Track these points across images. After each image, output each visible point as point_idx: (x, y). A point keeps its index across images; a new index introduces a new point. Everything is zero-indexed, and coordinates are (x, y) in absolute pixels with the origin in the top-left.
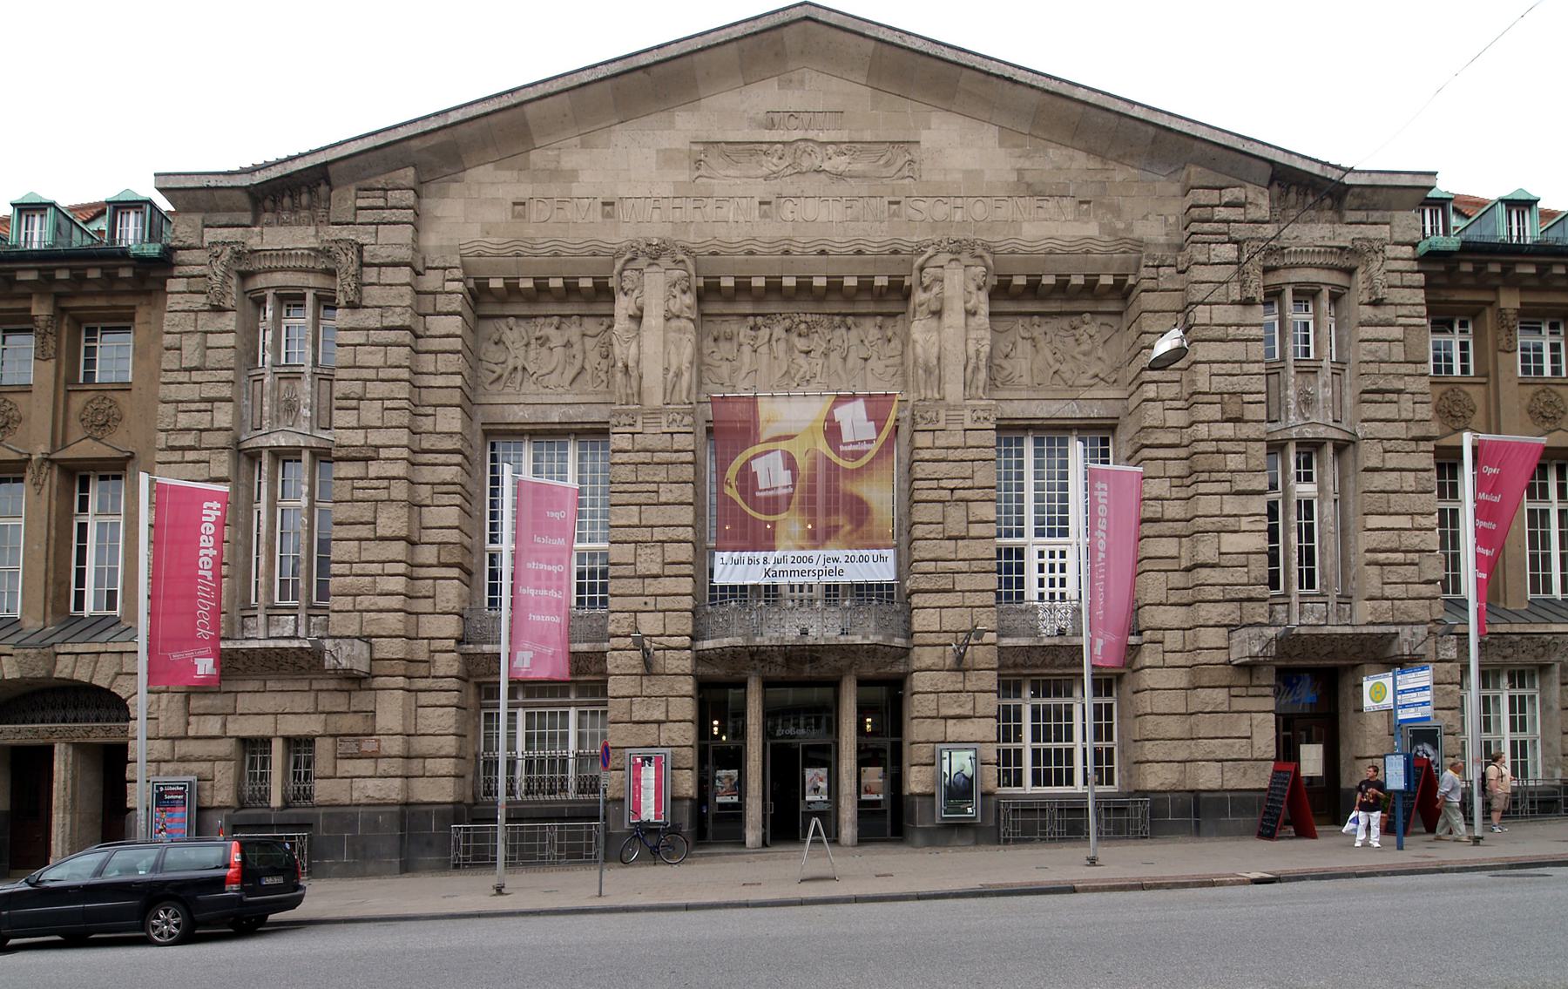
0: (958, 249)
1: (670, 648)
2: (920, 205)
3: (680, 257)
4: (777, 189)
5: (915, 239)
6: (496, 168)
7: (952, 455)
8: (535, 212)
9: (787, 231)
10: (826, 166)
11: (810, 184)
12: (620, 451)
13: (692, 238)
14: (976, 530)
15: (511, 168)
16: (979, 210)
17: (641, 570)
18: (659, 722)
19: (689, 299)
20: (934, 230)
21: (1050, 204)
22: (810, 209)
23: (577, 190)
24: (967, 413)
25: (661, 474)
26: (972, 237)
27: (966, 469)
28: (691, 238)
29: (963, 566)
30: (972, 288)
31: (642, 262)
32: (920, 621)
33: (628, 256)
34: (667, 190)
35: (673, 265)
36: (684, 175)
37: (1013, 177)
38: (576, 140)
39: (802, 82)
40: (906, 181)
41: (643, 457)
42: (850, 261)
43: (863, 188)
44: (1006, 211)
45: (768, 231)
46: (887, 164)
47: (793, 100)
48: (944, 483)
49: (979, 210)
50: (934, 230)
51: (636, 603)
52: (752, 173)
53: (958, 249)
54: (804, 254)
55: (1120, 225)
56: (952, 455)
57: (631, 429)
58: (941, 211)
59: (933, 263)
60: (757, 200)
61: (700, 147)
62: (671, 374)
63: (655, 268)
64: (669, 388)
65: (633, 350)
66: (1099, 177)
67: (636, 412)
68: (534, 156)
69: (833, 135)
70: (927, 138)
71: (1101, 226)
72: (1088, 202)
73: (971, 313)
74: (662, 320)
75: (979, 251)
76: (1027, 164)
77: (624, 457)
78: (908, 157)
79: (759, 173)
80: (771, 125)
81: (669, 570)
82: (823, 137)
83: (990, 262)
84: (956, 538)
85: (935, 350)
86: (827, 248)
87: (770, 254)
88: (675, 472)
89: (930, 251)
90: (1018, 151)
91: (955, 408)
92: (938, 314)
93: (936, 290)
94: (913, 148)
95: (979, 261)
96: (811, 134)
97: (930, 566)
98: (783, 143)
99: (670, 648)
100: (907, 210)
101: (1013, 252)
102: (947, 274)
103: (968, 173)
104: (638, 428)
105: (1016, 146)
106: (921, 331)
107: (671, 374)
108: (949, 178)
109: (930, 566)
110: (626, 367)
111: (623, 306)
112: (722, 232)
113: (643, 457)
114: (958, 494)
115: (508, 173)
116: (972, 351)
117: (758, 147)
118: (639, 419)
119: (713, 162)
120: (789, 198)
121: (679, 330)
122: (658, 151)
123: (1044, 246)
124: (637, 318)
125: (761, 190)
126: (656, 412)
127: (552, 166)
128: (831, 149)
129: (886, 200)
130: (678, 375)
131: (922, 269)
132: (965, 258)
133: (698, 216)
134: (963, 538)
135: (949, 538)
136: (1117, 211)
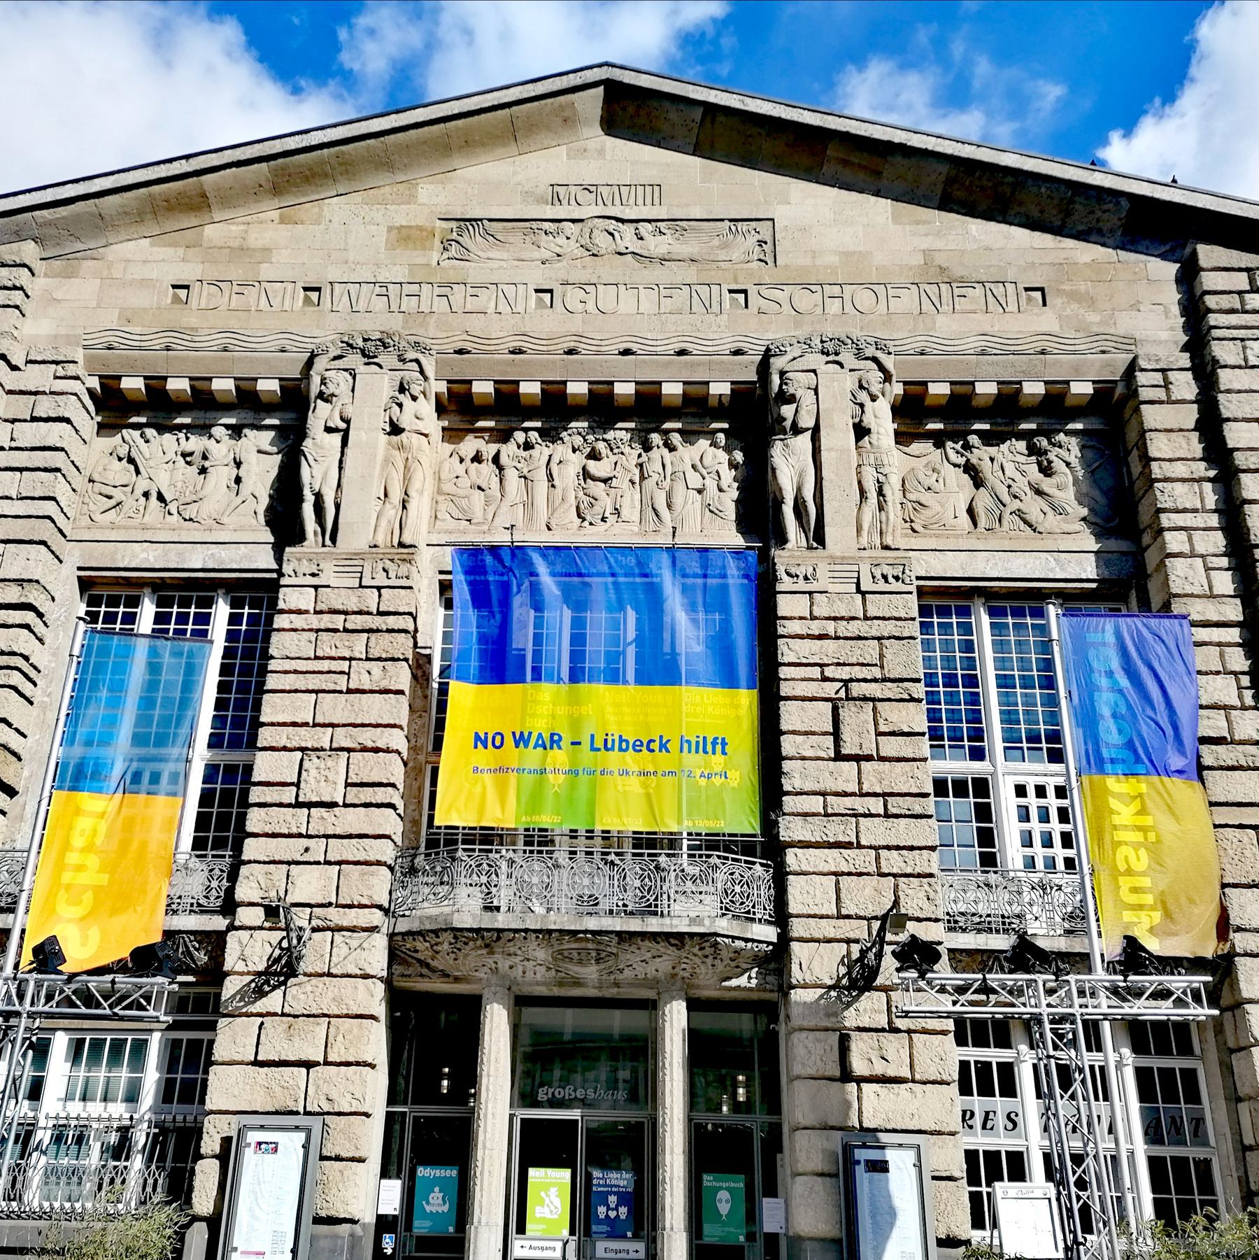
1: (341, 929)
2: (776, 294)
3: (411, 355)
4: (563, 275)
6: (152, 245)
7: (844, 628)
8: (202, 297)
9: (576, 324)
10: (635, 246)
11: (609, 268)
12: (291, 612)
14: (891, 747)
15: (175, 245)
17: (307, 795)
18: (308, 1065)
23: (266, 272)
25: (358, 645)
27: (870, 651)
29: (876, 805)
32: (800, 895)
38: (275, 215)
41: (327, 621)
42: (670, 363)
45: (549, 325)
46: (725, 246)
47: (589, 172)
48: (829, 672)
50: (798, 325)
51: (292, 849)
52: (524, 255)
54: (598, 353)
55: (1093, 318)
56: (844, 628)
57: (315, 581)
61: (454, 225)
68: (211, 232)
73: (861, 431)
75: (870, 351)
76: (939, 244)
77: (298, 621)
80: (556, 199)
81: (355, 795)
82: (629, 214)
83: (888, 362)
84: (857, 758)
86: (634, 347)
88: (381, 645)
90: (922, 228)
91: (843, 560)
94: (765, 228)
97: (816, 804)
98: (574, 221)
99: (341, 929)
103: (847, 255)
108: (818, 262)
109: (816, 804)
113: (327, 621)
114: (857, 689)
115: (169, 251)
117: (534, 225)
121: (401, 447)
122: (390, 229)
127: (236, 244)
128: (645, 229)
129: (725, 288)
132: (847, 357)
134: (869, 758)
135: (848, 758)
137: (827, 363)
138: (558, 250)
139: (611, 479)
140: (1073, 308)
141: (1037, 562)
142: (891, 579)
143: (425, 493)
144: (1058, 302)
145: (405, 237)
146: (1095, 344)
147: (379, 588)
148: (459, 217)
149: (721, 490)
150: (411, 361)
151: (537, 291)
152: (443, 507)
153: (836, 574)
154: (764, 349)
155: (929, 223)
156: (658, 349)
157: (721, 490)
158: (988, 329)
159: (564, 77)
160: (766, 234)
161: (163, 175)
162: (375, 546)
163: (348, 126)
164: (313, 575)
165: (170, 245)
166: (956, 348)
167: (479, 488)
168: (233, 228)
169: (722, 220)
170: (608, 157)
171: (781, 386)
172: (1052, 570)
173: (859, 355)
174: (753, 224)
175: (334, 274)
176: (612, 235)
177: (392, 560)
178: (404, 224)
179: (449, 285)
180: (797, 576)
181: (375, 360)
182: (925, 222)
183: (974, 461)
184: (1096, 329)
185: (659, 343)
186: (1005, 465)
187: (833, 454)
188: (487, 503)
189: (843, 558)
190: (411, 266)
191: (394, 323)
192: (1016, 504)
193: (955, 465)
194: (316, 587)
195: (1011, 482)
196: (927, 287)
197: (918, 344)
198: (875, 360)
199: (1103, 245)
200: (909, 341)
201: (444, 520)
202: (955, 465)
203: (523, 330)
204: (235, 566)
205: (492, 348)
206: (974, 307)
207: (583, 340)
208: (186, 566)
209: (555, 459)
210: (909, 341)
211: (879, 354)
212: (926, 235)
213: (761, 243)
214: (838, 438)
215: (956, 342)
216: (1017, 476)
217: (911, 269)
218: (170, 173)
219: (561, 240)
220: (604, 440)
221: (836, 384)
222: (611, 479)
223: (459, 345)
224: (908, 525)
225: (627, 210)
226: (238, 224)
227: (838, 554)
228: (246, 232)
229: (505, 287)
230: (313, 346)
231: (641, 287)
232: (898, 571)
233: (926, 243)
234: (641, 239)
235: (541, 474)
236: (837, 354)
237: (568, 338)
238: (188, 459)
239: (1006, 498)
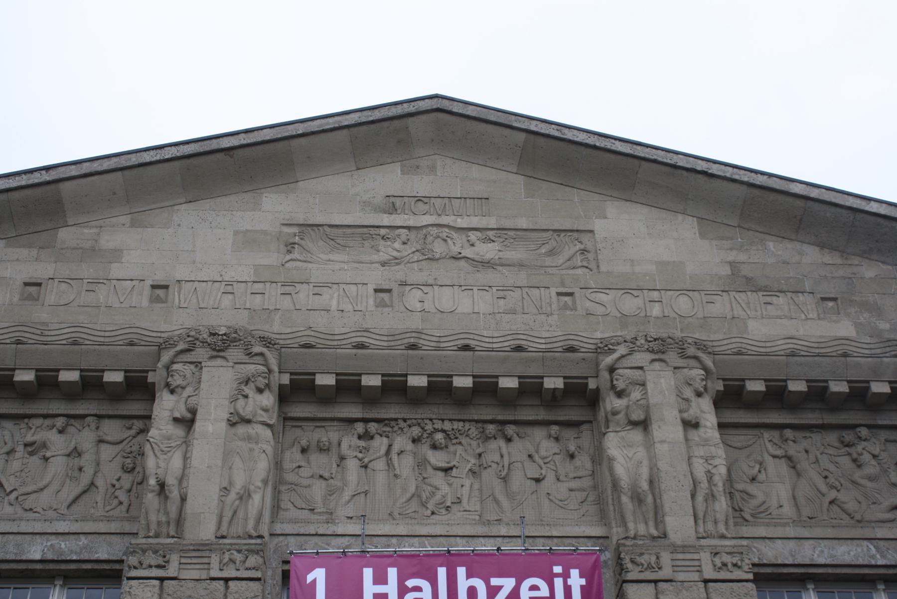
0: (659, 348)
2: (602, 297)
3: (257, 349)
4: (400, 276)
5: (599, 335)
8: (52, 295)
9: (415, 322)
10: (468, 252)
13: (276, 328)
15: (30, 246)
16: (683, 304)
19: (268, 399)
20: (624, 326)
21: (781, 300)
22: (445, 298)
24: (705, 557)
26: (678, 334)
28: (276, 327)
30: (688, 393)
31: (201, 354)
33: (181, 346)
34: (245, 273)
35: (246, 359)
36: (272, 258)
37: (726, 270)
38: (125, 219)
39: (432, 169)
40: (580, 271)
43: (522, 278)
44: (720, 306)
45: (388, 322)
46: (551, 253)
47: (421, 185)
49: (683, 304)
53: (659, 348)
54: (438, 349)
55: (884, 326)
57: (160, 573)
58: (630, 305)
59: (626, 362)
60: (371, 288)
61: (295, 230)
62: (233, 496)
63: (219, 362)
64: (228, 514)
65: (176, 462)
66: (841, 272)
67: (171, 549)
68: (64, 234)
69: (475, 222)
70: (599, 225)
71: (857, 325)
72: (834, 299)
73: (691, 425)
74: (224, 425)
75: (692, 351)
76: (742, 257)
78: (579, 246)
79: (375, 258)
80: (393, 209)
82: (461, 222)
83: (709, 363)
85: (645, 472)
86: (472, 343)
87: (389, 348)
89: (622, 350)
91: (686, 548)
92: (644, 424)
93: (636, 395)
94: (585, 238)
95: (693, 363)
96: (444, 220)
100: (584, 304)
101: (739, 353)
102: (650, 377)
103: (662, 265)
104: (171, 571)
105: (722, 238)
106: (623, 452)
107: (233, 496)
108: (638, 269)
110: (162, 485)
111: (166, 406)
112: (320, 322)
115: (24, 252)
116: (700, 473)
117: (372, 231)
118: (174, 559)
119: (310, 245)
120: (417, 286)
121: (249, 438)
122: (236, 233)
123: (782, 346)
124: (187, 422)
125: (377, 277)
126: (203, 548)
128: (473, 236)
129: (553, 291)
130: (245, 496)
131: (612, 370)
132: (672, 357)
133: (286, 303)
136: (877, 311)
137: (653, 360)
138: (395, 254)
139: (451, 468)
140: (864, 317)
141: (859, 550)
142: (730, 565)
143: (270, 484)
144: (852, 310)
145: (248, 240)
146: (888, 349)
147: (226, 580)
148: (301, 223)
149: (558, 479)
150: (256, 354)
151: (376, 291)
152: (285, 497)
153: (679, 563)
155: (732, 239)
156: (495, 346)
157: (558, 479)
158: (793, 333)
159: (399, 107)
160: (589, 245)
161: (23, 183)
162: (223, 537)
163: (200, 143)
164: (159, 567)
165: (24, 246)
166: (768, 350)
167: (321, 477)
168: (86, 231)
169: (548, 230)
170: (439, 174)
172: (873, 557)
173: (683, 355)
174: (576, 235)
175: (181, 273)
176: (445, 241)
177: (239, 551)
178: (250, 228)
179: (292, 284)
180: (642, 565)
182: (727, 239)
183: (791, 452)
184: (887, 336)
185: (495, 340)
186: (819, 456)
187: (665, 447)
188: (331, 492)
189: (684, 546)
190: (257, 268)
191: (241, 320)
192: (833, 494)
193: (774, 457)
194: (162, 579)
195: (826, 473)
196: (737, 295)
197: (734, 346)
198: (696, 358)
199: (884, 263)
200: (725, 342)
201: (287, 510)
202: (774, 457)
203: (365, 326)
204: (75, 558)
205: (335, 343)
206: (779, 313)
207: (423, 336)
208: (24, 558)
209: (396, 448)
210: (725, 342)
211: (700, 354)
212: (731, 249)
213: (584, 251)
214: (666, 429)
215: (768, 344)
216: (832, 468)
217: (720, 278)
218: (30, 182)
219: (397, 245)
220: (443, 431)
221: (662, 380)
222: (451, 468)
223: (303, 340)
224: (737, 514)
225: (459, 220)
226: (91, 227)
227: (679, 543)
228: (98, 234)
229: (346, 287)
230: (161, 340)
231: (475, 289)
232: (735, 560)
233: (732, 256)
234: (473, 245)
235: (380, 464)
237: (408, 335)
238: (30, 449)
239: (824, 488)
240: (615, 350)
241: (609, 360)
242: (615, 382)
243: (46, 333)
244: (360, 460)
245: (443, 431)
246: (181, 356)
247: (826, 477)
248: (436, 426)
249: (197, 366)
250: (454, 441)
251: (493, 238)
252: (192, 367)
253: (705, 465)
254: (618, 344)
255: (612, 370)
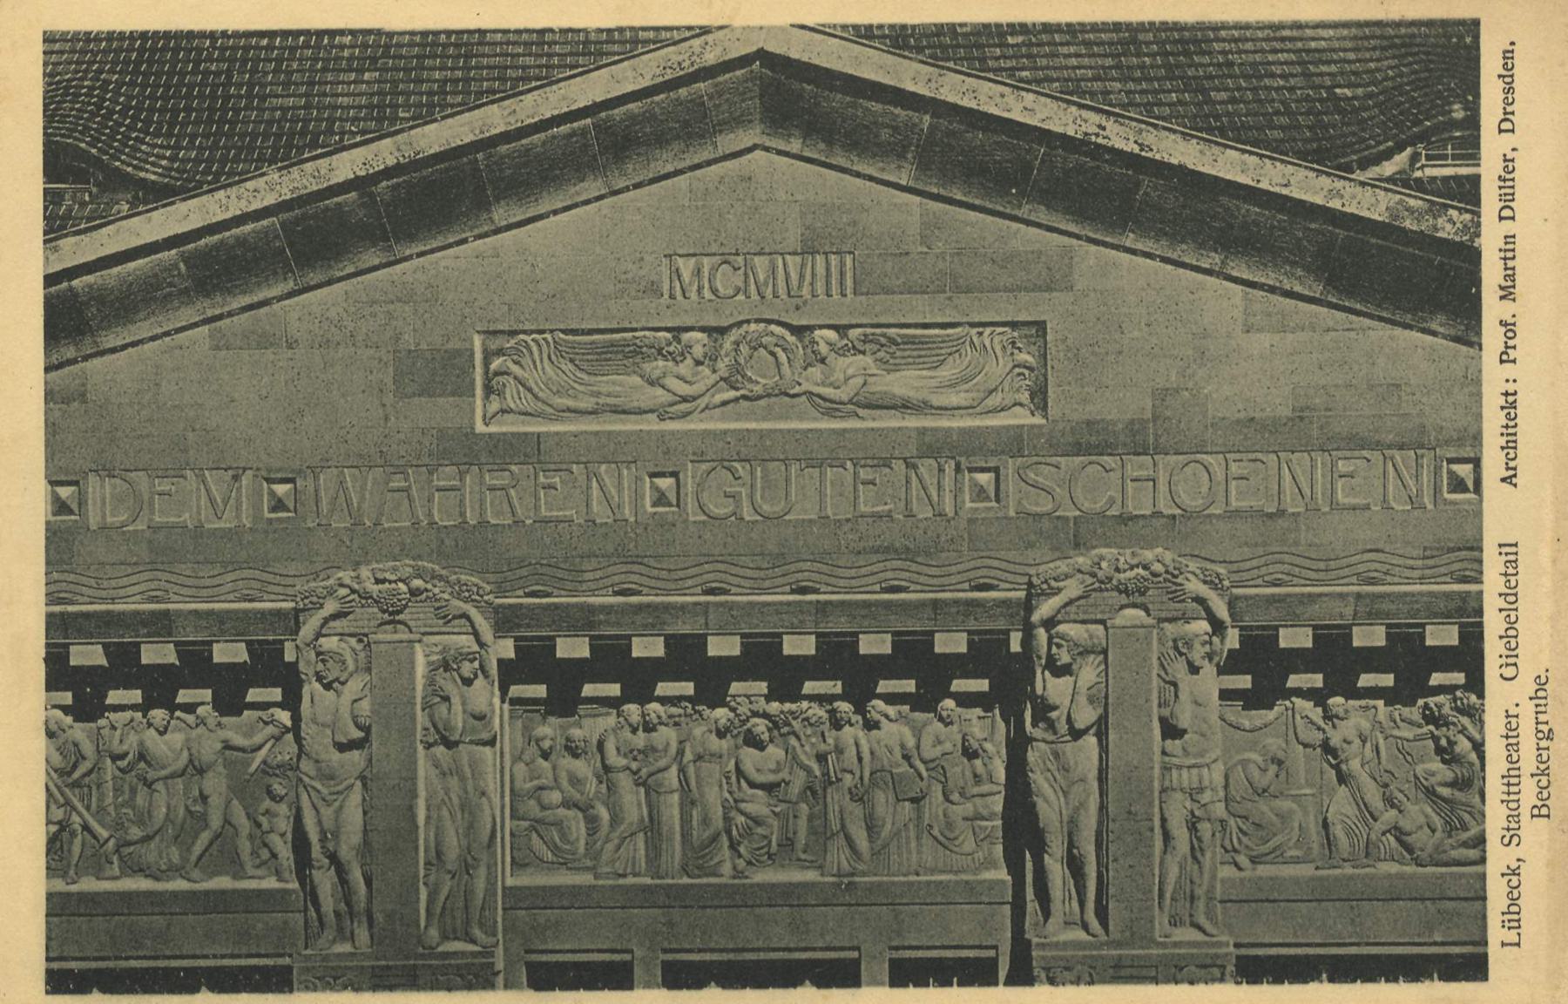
138: (684, 389)
154: (1026, 579)
171: (1049, 649)
181: (400, 617)
183: (1335, 741)
195: (1386, 778)
219: (685, 368)
220: (765, 715)
236: (1143, 594)
239: (1376, 802)
240: (1060, 590)
241: (1045, 609)
242: (1054, 650)
243: (105, 584)
244: (635, 773)
245: (765, 715)
246: (332, 624)
247: (1386, 786)
248: (755, 707)
249: (360, 641)
250: (785, 730)
251: (860, 346)
252: (353, 641)
253: (1188, 804)
254: (1067, 577)
255: (1049, 623)
